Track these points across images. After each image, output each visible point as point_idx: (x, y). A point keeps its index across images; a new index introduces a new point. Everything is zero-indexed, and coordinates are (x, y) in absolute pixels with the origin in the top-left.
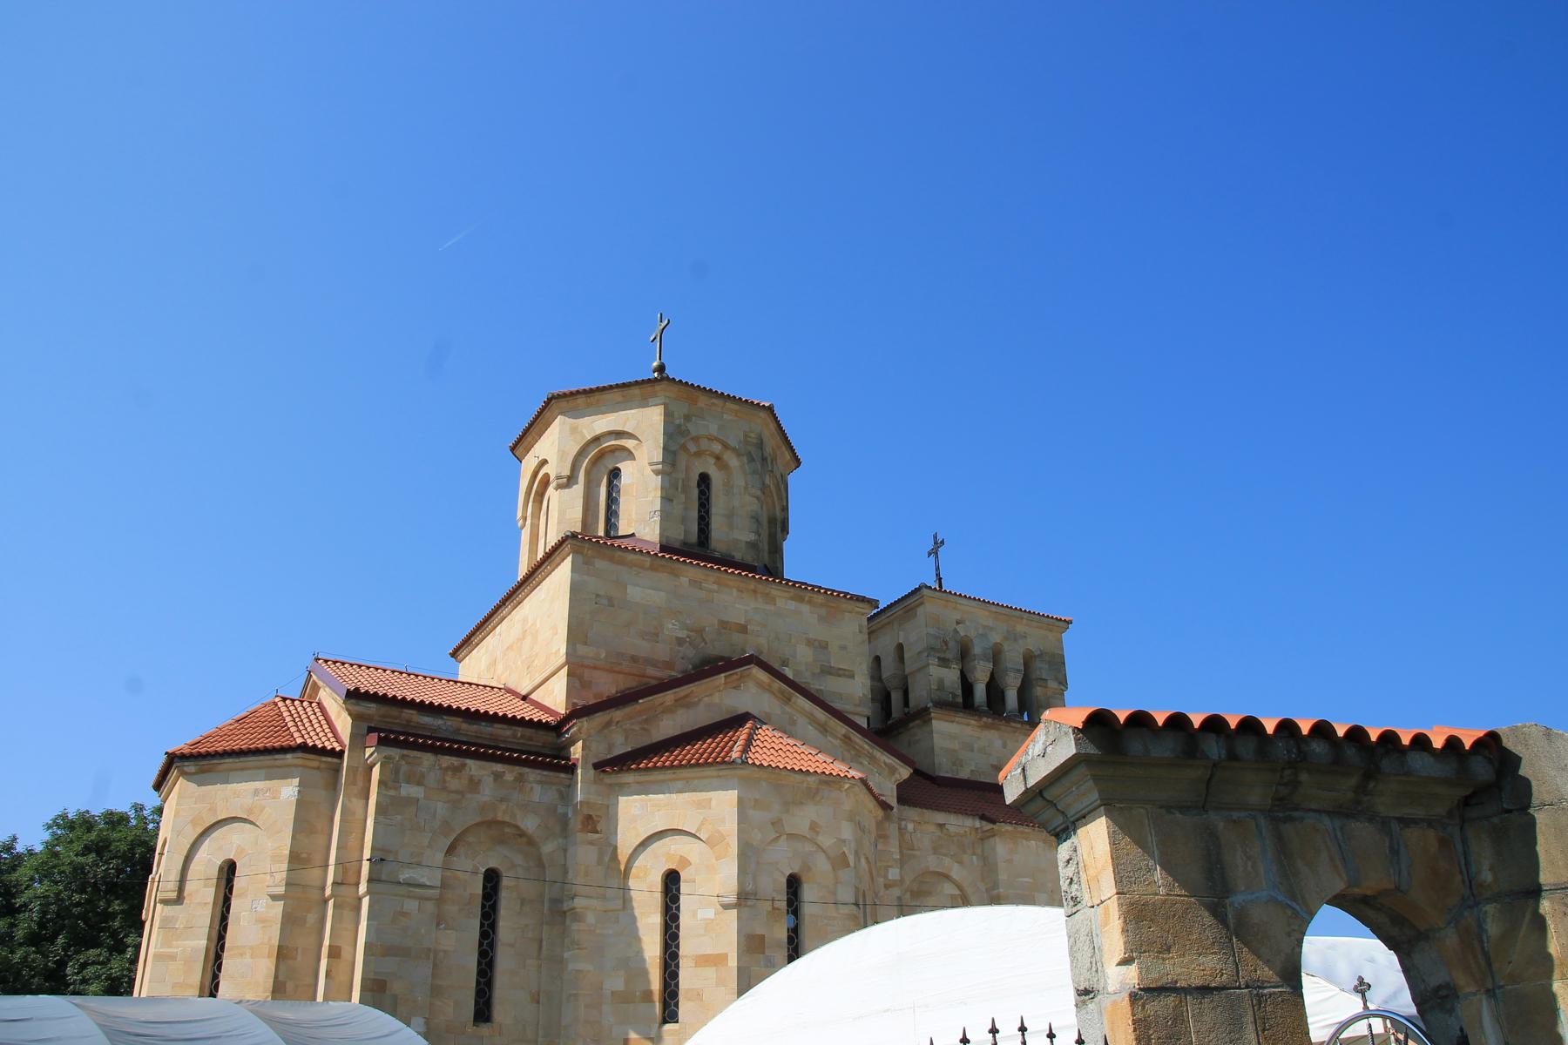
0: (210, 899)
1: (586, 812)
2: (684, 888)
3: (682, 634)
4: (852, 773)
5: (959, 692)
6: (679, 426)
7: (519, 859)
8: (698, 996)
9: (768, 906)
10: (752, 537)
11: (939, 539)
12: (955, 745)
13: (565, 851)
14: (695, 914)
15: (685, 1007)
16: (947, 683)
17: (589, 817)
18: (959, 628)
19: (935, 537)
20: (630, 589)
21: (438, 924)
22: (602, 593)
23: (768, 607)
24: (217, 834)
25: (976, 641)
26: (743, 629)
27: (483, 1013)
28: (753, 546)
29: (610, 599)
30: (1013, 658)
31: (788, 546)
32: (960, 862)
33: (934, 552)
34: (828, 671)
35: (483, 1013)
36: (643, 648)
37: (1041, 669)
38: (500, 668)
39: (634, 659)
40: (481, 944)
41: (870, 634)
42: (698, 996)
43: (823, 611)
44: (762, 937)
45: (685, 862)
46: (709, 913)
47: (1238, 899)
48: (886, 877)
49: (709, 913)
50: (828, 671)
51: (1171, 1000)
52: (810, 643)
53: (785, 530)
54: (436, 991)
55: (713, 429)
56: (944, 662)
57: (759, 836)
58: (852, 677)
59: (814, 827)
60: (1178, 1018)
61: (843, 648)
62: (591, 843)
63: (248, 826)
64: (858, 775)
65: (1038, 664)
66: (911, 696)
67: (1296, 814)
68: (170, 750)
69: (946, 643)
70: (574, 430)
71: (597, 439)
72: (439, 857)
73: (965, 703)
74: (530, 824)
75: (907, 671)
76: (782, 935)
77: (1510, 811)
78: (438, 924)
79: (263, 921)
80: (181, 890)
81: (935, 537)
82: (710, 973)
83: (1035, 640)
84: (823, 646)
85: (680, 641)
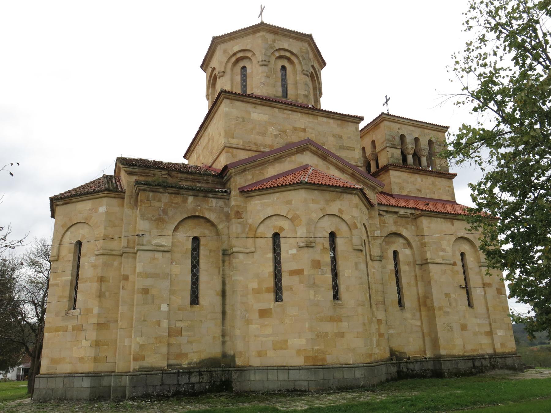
0: (71, 259)
1: (236, 209)
2: (282, 240)
3: (277, 133)
4: (356, 186)
6: (270, 45)
7: (207, 232)
8: (291, 288)
9: (321, 247)
10: (306, 93)
12: (400, 181)
13: (228, 228)
14: (287, 252)
15: (285, 295)
16: (395, 155)
17: (238, 212)
18: (399, 131)
20: (252, 114)
21: (172, 263)
22: (239, 116)
23: (315, 121)
24: (73, 228)
25: (407, 137)
26: (304, 130)
27: (195, 300)
28: (306, 96)
29: (244, 119)
30: (424, 144)
31: (322, 100)
32: (407, 229)
34: (342, 148)
35: (195, 300)
36: (260, 139)
38: (201, 158)
39: (255, 144)
40: (192, 271)
41: (361, 137)
42: (291, 288)
43: (339, 122)
44: (319, 261)
45: (282, 229)
46: (294, 251)
48: (374, 234)
49: (294, 251)
50: (342, 148)
52: (334, 136)
53: (321, 93)
54: (172, 292)
55: (286, 46)
56: (393, 147)
57: (315, 215)
58: (354, 150)
59: (340, 211)
61: (349, 138)
62: (239, 223)
63: (86, 226)
64: (360, 187)
65: (435, 146)
66: (379, 162)
68: (52, 195)
69: (394, 137)
70: (225, 51)
71: (235, 54)
72: (171, 233)
74: (212, 217)
75: (377, 151)
76: (329, 260)
78: (172, 263)
79: (94, 266)
80: (58, 256)
82: (296, 278)
83: (433, 136)
84: (340, 137)
85: (276, 136)
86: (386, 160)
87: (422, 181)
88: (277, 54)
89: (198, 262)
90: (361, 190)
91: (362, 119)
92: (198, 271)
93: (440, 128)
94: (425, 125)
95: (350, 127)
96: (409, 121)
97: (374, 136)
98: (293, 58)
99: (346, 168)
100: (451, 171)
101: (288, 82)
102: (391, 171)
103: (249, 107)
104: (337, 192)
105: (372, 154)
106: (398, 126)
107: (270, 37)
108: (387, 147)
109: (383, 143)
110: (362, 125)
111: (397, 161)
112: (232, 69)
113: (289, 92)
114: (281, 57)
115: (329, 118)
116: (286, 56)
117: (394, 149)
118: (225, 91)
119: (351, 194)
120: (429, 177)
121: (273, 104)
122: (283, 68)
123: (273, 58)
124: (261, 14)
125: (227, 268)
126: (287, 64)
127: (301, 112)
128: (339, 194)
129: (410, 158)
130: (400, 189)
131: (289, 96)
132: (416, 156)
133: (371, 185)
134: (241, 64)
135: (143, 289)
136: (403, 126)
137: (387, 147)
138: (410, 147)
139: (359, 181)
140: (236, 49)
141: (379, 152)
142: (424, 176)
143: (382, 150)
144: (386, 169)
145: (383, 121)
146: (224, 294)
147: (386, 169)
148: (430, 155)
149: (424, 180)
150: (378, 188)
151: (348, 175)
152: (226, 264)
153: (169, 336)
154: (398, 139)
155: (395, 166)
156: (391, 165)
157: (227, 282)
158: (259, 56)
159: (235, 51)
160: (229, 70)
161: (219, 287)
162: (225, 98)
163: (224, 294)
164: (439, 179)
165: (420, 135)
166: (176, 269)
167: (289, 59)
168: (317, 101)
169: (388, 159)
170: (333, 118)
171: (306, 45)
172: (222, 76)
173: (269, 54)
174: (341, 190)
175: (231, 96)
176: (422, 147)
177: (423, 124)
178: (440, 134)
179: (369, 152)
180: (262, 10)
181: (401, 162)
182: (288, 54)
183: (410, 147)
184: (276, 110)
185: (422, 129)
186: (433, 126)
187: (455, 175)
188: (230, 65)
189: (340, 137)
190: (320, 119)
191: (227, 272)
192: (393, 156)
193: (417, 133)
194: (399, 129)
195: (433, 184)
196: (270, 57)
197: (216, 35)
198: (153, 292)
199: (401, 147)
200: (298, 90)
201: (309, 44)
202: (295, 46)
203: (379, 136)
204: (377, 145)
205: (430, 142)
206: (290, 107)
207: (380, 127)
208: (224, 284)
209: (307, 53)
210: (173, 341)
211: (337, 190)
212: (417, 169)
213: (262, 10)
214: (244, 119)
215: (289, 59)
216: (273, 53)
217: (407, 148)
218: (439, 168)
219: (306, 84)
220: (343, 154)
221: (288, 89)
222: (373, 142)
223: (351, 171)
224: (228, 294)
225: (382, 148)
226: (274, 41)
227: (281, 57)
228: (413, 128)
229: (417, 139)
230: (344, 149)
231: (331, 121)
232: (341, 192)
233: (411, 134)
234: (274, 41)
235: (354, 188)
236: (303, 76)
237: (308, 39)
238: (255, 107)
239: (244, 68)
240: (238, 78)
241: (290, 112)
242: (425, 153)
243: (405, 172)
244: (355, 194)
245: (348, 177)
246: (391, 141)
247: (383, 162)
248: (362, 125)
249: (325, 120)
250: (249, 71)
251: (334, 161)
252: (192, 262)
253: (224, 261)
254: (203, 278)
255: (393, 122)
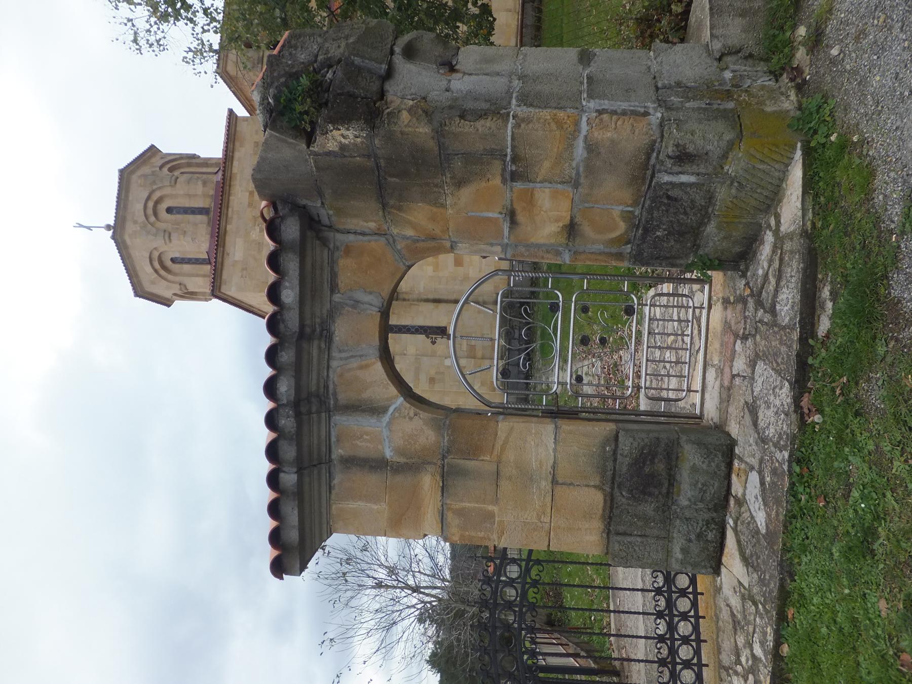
10: (200, 183)
23: (238, 178)
27: (442, 331)
28: (205, 183)
29: (243, 269)
40: (412, 333)
47: (388, 454)
51: (450, 516)
53: (194, 156)
55: (140, 207)
60: (460, 513)
67: (331, 387)
71: (156, 271)
77: (322, 203)
88: (152, 219)
89: (404, 327)
92: (413, 327)
98: (155, 196)
101: (187, 205)
103: (228, 262)
107: (130, 227)
112: (175, 274)
113: (201, 206)
114: (155, 214)
116: (153, 208)
118: (212, 291)
121: (222, 231)
122: (169, 210)
123: (158, 224)
124: (89, 228)
125: (410, 297)
126: (164, 206)
127: (229, 195)
131: (207, 206)
134: (169, 263)
135: (430, 383)
140: (149, 269)
146: (437, 301)
152: (406, 297)
153: (474, 357)
157: (425, 297)
158: (159, 243)
159: (152, 270)
160: (178, 279)
161: (431, 306)
162: (220, 291)
163: (437, 301)
166: (411, 350)
167: (157, 203)
168: (206, 162)
171: (134, 177)
172: (185, 286)
173: (154, 230)
175: (217, 284)
180: (81, 226)
182: (151, 204)
184: (228, 227)
188: (170, 277)
190: (235, 170)
191: (415, 296)
196: (158, 229)
197: (132, 293)
198: (432, 372)
200: (199, 194)
201: (133, 172)
202: (139, 194)
206: (224, 210)
208: (427, 301)
209: (145, 176)
210: (479, 354)
213: (81, 226)
214: (243, 269)
215: (157, 203)
216: (152, 225)
219: (189, 181)
221: (196, 206)
224: (437, 297)
226: (135, 222)
227: (155, 214)
234: (135, 222)
236: (178, 185)
237: (126, 175)
238: (228, 254)
239: (173, 260)
240: (187, 268)
241: (230, 210)
249: (235, 163)
250: (177, 255)
252: (404, 333)
253: (404, 300)
254: (420, 321)
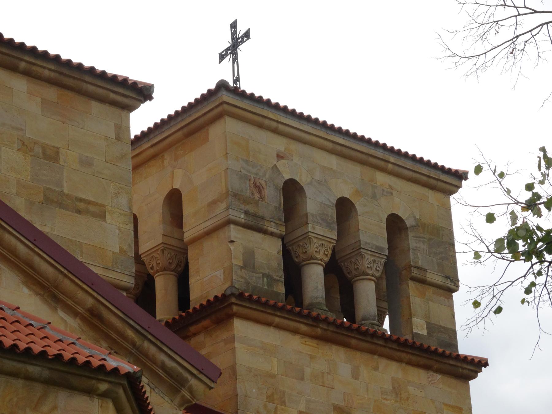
4: (112, 363)
5: (280, 275)
11: (241, 30)
12: (273, 366)
16: (260, 259)
18: (280, 164)
19: (234, 26)
25: (309, 192)
30: (371, 230)
33: (233, 49)
34: (55, 200)
37: (417, 250)
43: (51, 93)
50: (55, 200)
52: (25, 146)
56: (254, 225)
58: (102, 216)
61: (86, 163)
65: (412, 241)
69: (259, 188)
73: (285, 305)
75: (188, 235)
81: (234, 26)
83: (405, 201)
84: (51, 156)
86: (219, 274)
87: (356, 376)
90: (132, 381)
91: (143, 93)
93: (433, 173)
94: (380, 153)
95: (96, 120)
96: (322, 133)
97: (179, 173)
99: (68, 285)
100: (465, 348)
102: (238, 325)
104: (28, 378)
105: (165, 247)
106: (279, 144)
108: (229, 222)
109: (213, 204)
110: (141, 119)
111: (263, 284)
115: (13, 69)
117: (258, 236)
119: (90, 392)
120: (383, 363)
128: (39, 388)
129: (315, 280)
130: (270, 398)
132: (341, 278)
133: (163, 367)
136: (295, 146)
137: (229, 222)
138: (320, 237)
139: (117, 346)
141: (194, 240)
142: (367, 356)
143: (209, 233)
144: (219, 311)
145: (220, 116)
147: (219, 311)
148: (394, 279)
149: (364, 372)
150: (193, 382)
151: (75, 314)
154: (273, 199)
155: (258, 302)
156: (241, 296)
164: (418, 376)
165: (358, 193)
169: (229, 272)
170: (27, 74)
174: (46, 373)
176: (364, 238)
177: (372, 151)
178: (432, 196)
179: (153, 234)
181: (281, 289)
183: (320, 237)
185: (368, 172)
186: (409, 164)
187: (481, 364)
189: (51, 156)
192: (249, 263)
193: (346, 181)
194: (280, 157)
195: (397, 390)
199: (282, 230)
203: (200, 175)
204: (187, 210)
205: (395, 225)
207: (206, 139)
211: (33, 369)
212: (341, 327)
217: (306, 237)
218: (420, 327)
220: (57, 226)
222: (174, 200)
223: (90, 301)
225: (209, 225)
228: (333, 161)
229: (344, 207)
230: (61, 205)
231: (19, 84)
232: (48, 382)
233: (325, 183)
235: (102, 367)
242: (372, 264)
243: (295, 332)
244: (104, 395)
245: (73, 323)
246: (246, 201)
247: (207, 280)
248: (141, 119)
251: (21, 248)
255: (260, 126)
